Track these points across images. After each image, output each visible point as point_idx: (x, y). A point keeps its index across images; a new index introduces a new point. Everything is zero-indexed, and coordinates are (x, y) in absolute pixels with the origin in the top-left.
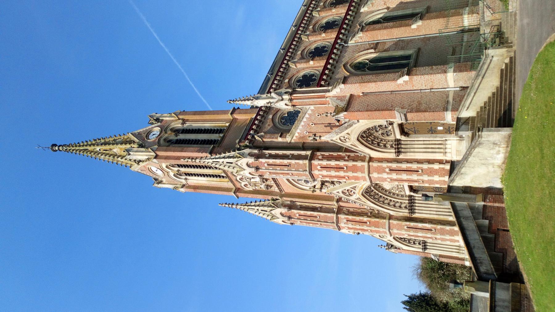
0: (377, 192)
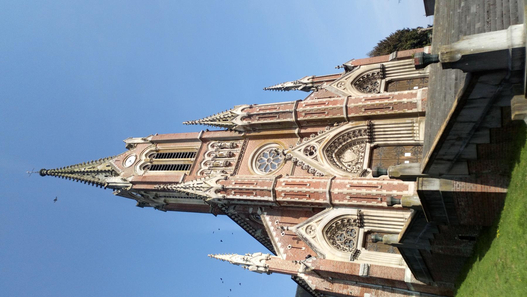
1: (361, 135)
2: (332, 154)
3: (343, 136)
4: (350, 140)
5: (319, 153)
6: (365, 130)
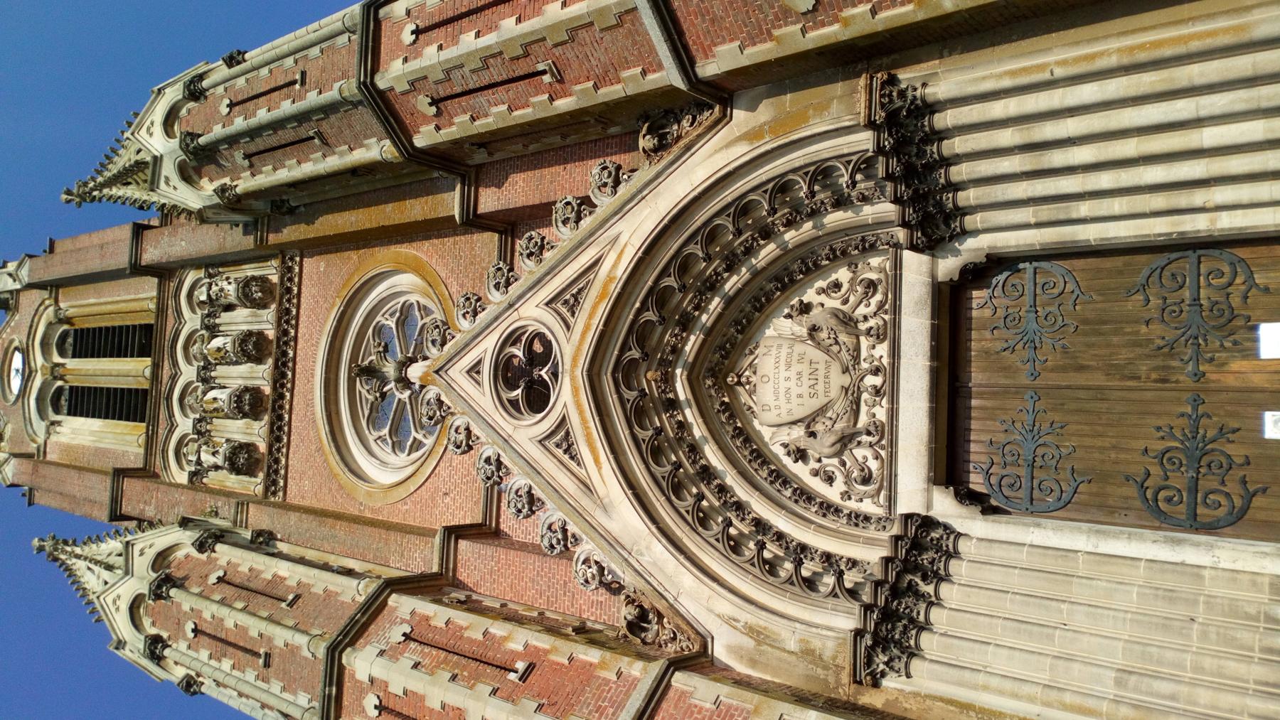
0: (699, 431)
1: (841, 202)
2: (668, 380)
3: (710, 234)
4: (768, 251)
5: (569, 396)
6: (865, 165)
